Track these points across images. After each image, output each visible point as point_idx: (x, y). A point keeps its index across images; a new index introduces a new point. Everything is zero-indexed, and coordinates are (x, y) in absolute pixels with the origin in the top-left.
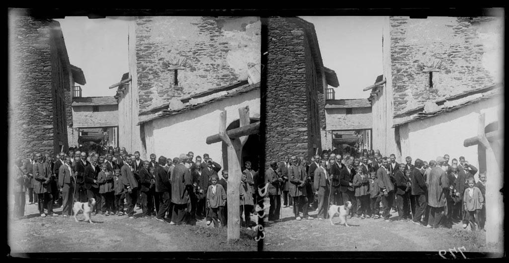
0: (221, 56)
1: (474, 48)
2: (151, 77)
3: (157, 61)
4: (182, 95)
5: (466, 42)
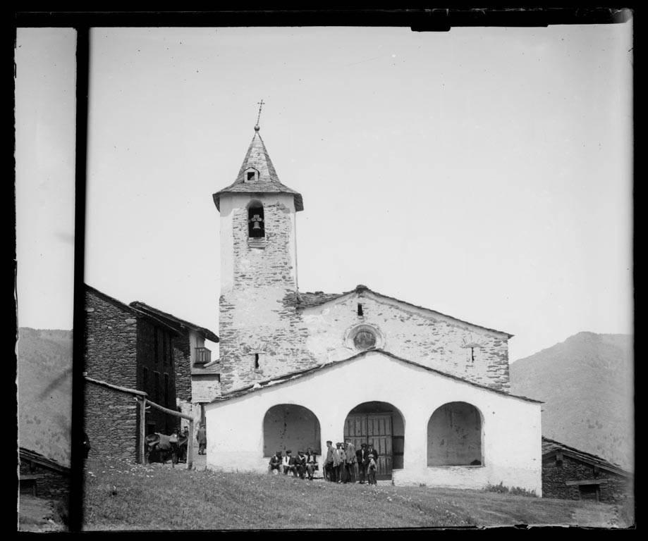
1: (299, 331)
2: (232, 360)
3: (239, 346)
5: (292, 326)
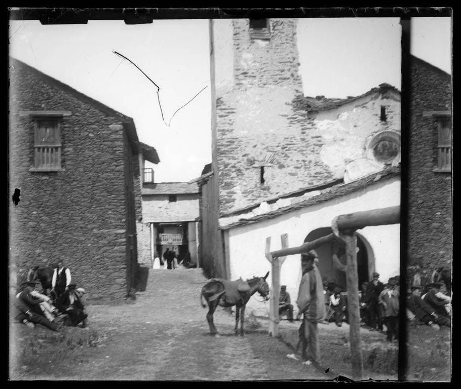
0: (313, 151)
1: (311, 140)
2: (234, 175)
3: (241, 158)
4: (269, 195)
5: (304, 133)
